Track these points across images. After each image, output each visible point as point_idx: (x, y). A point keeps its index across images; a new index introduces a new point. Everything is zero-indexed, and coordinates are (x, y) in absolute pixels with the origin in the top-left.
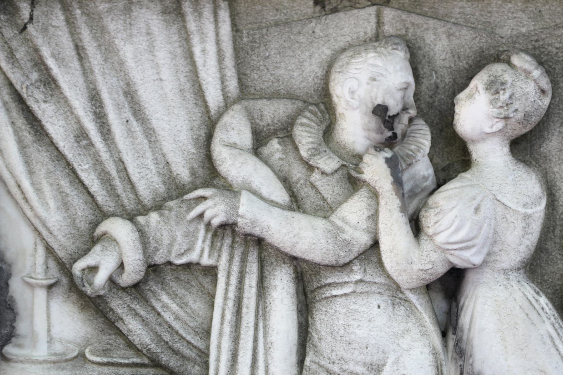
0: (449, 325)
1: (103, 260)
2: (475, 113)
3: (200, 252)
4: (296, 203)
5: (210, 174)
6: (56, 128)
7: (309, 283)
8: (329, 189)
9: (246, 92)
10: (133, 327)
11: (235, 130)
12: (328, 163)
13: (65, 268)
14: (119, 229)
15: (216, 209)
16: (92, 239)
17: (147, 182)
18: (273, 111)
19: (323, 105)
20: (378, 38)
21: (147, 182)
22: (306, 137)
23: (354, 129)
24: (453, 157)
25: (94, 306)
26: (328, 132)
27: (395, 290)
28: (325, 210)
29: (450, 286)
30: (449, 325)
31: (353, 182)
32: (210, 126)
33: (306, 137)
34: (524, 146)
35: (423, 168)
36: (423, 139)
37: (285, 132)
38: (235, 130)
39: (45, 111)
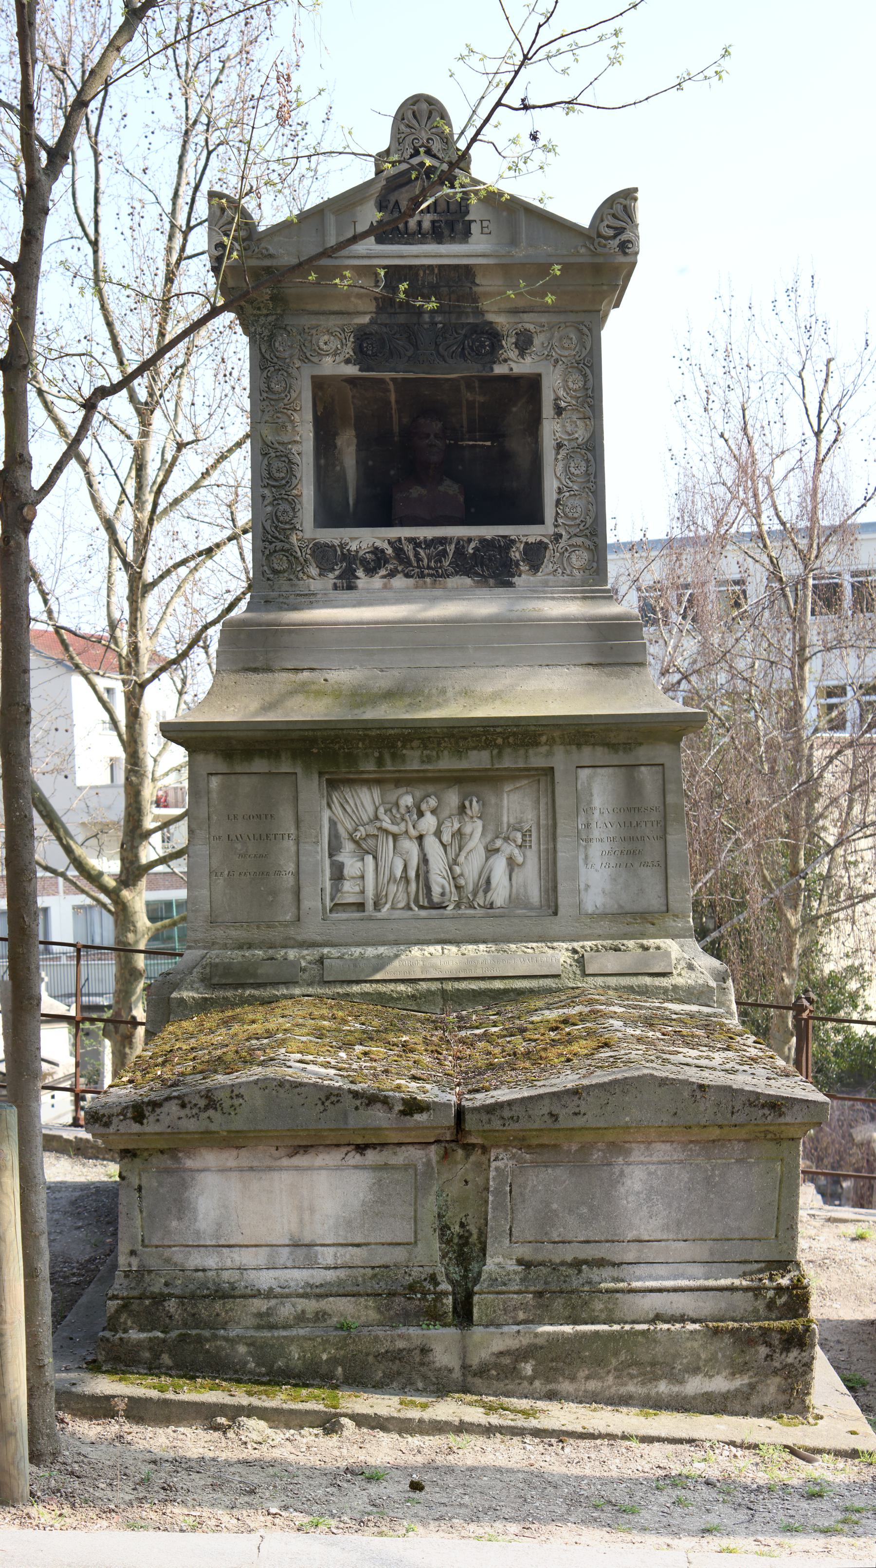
0: (421, 845)
1: (359, 835)
2: (424, 807)
3: (376, 832)
4: (393, 823)
5: (377, 818)
6: (349, 810)
7: (395, 837)
8: (399, 821)
9: (383, 803)
10: (364, 846)
11: (381, 810)
12: (398, 816)
13: (351, 835)
14: (361, 828)
15: (378, 824)
16: (356, 830)
17: (365, 819)
18: (388, 806)
19: (397, 805)
20: (407, 793)
21: (365, 819)
22: (394, 811)
23: (403, 810)
24: (421, 814)
25: (356, 842)
26: (398, 810)
27: (410, 838)
28: (398, 824)
29: (420, 838)
30: (421, 845)
31: (403, 819)
32: (377, 809)
33: (394, 811)
34: (433, 812)
35: (415, 817)
36: (415, 810)
37: (390, 810)
38: (381, 810)
39: (347, 807)
